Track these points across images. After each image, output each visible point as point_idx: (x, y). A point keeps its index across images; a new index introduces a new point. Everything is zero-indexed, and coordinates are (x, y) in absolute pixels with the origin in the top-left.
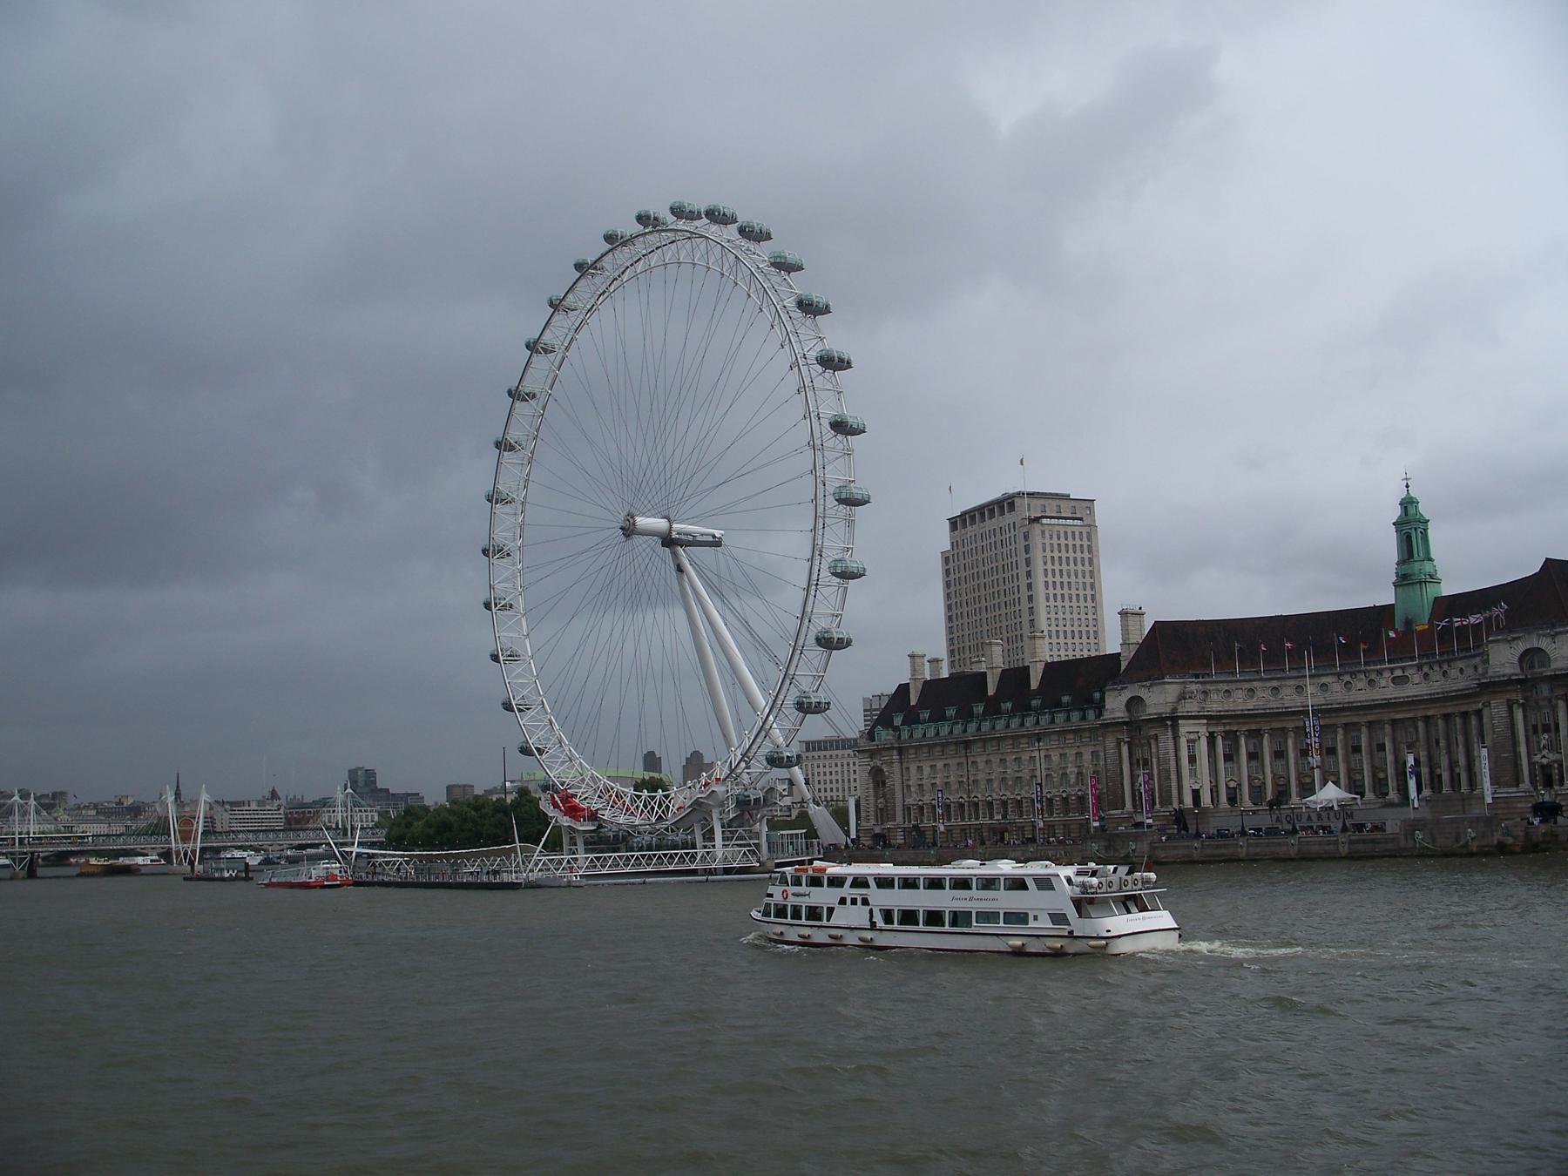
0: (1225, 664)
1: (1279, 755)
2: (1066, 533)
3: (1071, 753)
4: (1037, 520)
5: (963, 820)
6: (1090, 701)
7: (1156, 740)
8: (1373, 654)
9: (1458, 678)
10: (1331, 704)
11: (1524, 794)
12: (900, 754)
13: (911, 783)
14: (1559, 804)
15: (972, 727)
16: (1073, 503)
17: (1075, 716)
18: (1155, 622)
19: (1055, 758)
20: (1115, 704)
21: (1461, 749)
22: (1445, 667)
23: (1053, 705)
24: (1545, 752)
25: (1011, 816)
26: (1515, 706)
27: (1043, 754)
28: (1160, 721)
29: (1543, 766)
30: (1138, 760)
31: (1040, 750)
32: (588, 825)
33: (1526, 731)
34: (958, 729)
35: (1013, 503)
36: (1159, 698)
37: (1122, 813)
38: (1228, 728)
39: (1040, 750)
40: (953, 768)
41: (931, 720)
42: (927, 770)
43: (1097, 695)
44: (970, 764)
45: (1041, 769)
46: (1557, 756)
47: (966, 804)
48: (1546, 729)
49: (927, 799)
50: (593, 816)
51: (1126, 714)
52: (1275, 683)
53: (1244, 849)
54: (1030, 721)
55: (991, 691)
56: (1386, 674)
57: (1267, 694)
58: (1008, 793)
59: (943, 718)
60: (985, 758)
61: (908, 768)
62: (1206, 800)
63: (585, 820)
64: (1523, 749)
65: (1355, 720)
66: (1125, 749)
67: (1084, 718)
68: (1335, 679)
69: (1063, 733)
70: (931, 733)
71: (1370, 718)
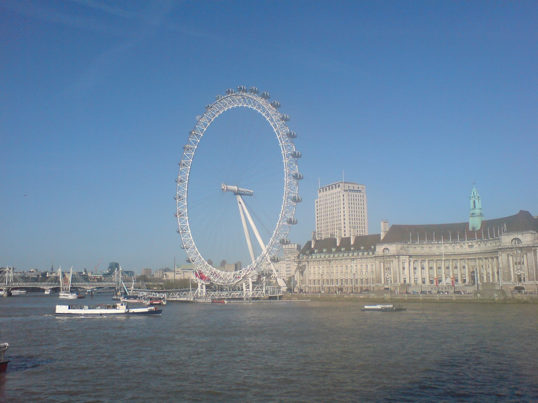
0: (414, 239)
1: (431, 268)
2: (356, 195)
3: (364, 265)
4: (347, 190)
5: (328, 284)
6: (370, 248)
7: (392, 262)
8: (462, 238)
9: (490, 246)
10: (448, 253)
11: (512, 284)
12: (308, 263)
13: (311, 272)
14: (523, 287)
16: (359, 186)
17: (366, 253)
18: (393, 225)
19: (359, 266)
20: (379, 249)
21: (490, 269)
22: (486, 243)
23: (357, 249)
24: (519, 271)
26: (510, 256)
27: (355, 265)
28: (394, 256)
29: (518, 275)
30: (386, 268)
31: (354, 264)
32: (207, 282)
33: (513, 264)
34: (327, 256)
35: (339, 186)
36: (393, 248)
37: (381, 285)
38: (415, 259)
39: (354, 264)
40: (325, 268)
41: (318, 252)
42: (317, 268)
43: (373, 247)
44: (331, 267)
46: (523, 272)
47: (329, 280)
48: (519, 263)
49: (317, 277)
50: (209, 280)
51: (383, 254)
52: (430, 246)
53: (422, 297)
54: (351, 254)
55: (338, 245)
56: (466, 244)
57: (428, 249)
58: (343, 277)
59: (322, 252)
60: (336, 265)
62: (408, 281)
63: (206, 281)
64: (512, 269)
65: (456, 258)
66: (382, 264)
67: (368, 254)
68: (450, 245)
69: (361, 258)
70: (318, 256)
71: (461, 258)
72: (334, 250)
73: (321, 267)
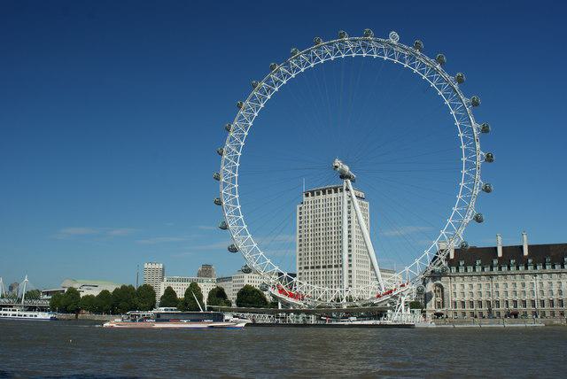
15: (495, 270)
19: (545, 283)
25: (520, 307)
27: (538, 281)
42: (467, 286)
45: (537, 288)
49: (466, 298)
55: (500, 254)
61: (454, 285)
72: (495, 262)
73: (475, 284)
